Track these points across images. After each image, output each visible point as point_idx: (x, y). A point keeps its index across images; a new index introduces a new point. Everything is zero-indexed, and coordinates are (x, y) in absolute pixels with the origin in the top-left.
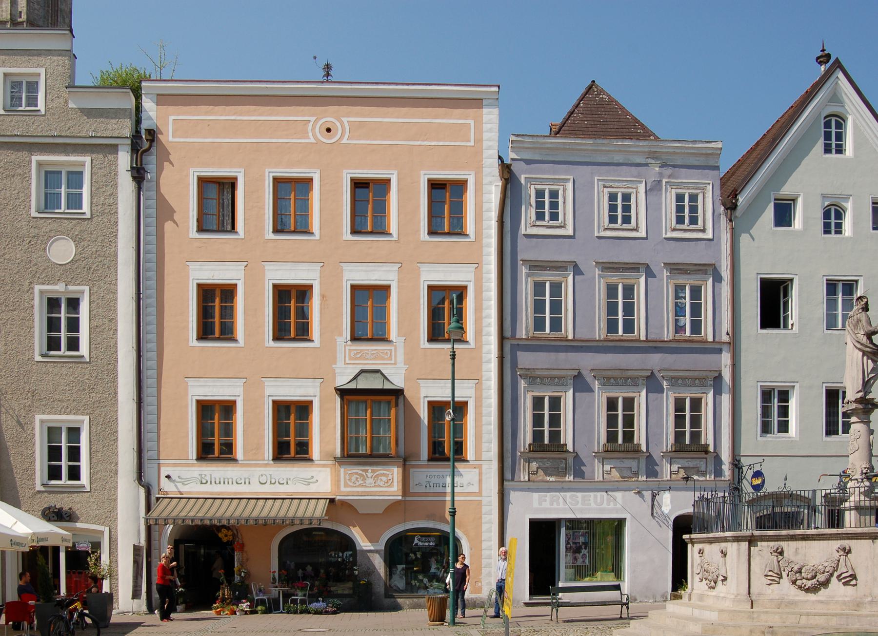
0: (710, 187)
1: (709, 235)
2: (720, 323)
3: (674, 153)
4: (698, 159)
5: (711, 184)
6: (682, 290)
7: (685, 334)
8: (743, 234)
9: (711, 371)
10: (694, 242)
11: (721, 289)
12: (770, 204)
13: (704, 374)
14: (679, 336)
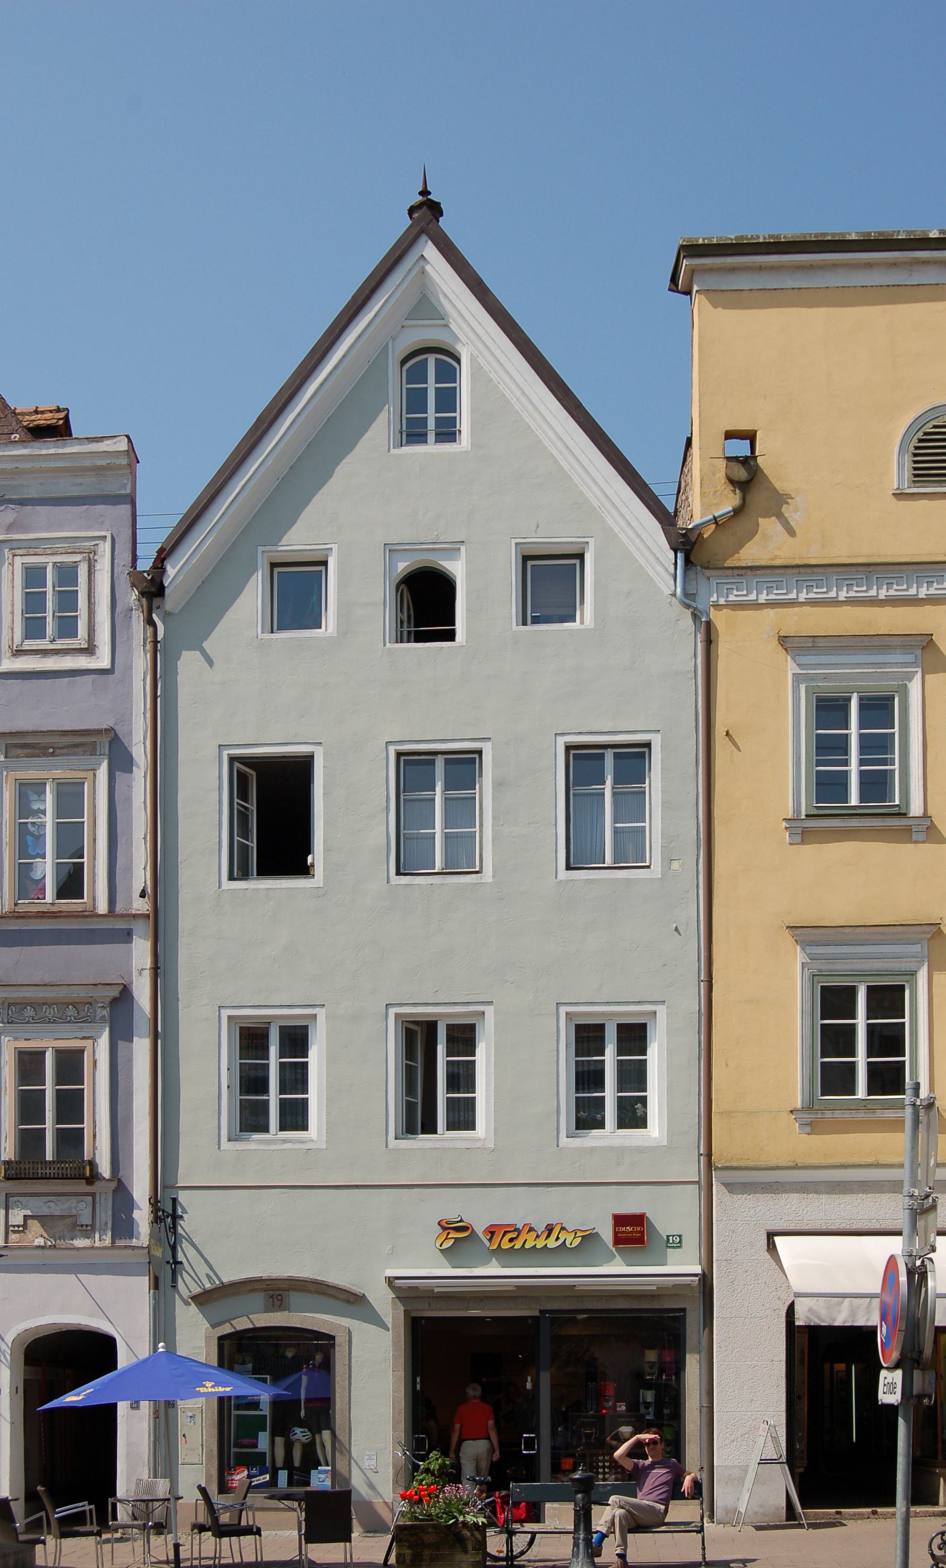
0: (108, 545)
1: (103, 662)
2: (129, 869)
3: (17, 472)
4: (79, 480)
5: (109, 539)
6: (39, 796)
7: (44, 898)
8: (184, 653)
9: (96, 985)
10: (67, 679)
11: (130, 787)
12: (254, 577)
13: (82, 993)
14: (26, 905)
